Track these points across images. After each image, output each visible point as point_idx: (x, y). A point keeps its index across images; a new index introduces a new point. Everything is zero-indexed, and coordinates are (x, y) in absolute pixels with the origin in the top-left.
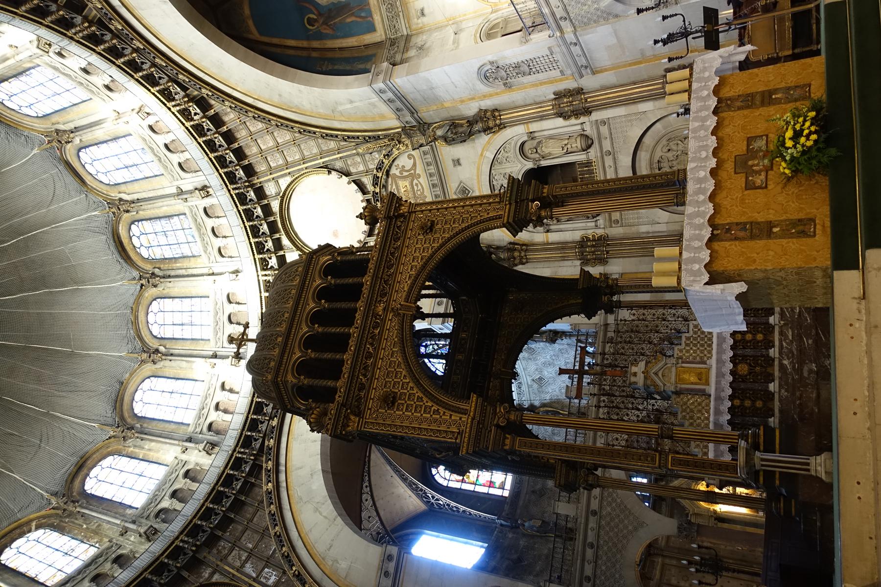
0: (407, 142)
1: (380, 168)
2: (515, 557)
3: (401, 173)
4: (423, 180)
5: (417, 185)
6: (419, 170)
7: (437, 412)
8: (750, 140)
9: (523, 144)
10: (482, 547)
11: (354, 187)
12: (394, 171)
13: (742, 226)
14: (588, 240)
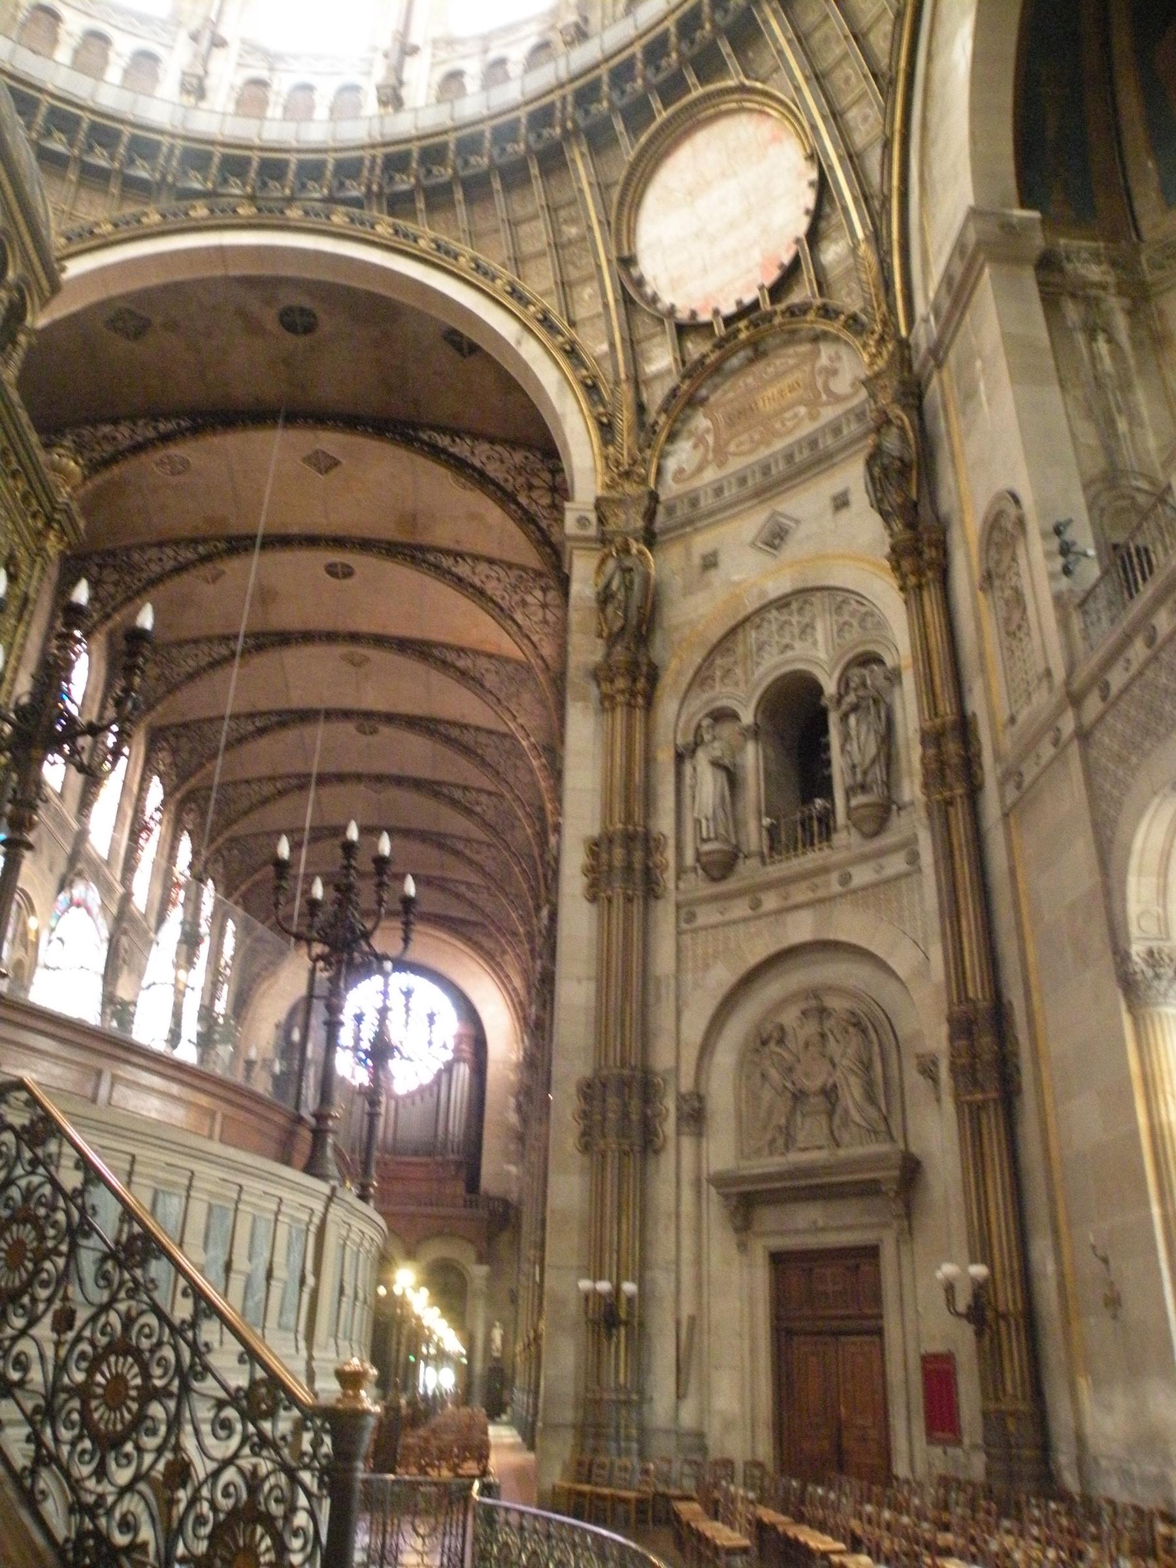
0: (881, 363)
6: (829, 413)
9: (869, 660)
11: (786, 259)
12: (826, 351)
14: (648, 853)
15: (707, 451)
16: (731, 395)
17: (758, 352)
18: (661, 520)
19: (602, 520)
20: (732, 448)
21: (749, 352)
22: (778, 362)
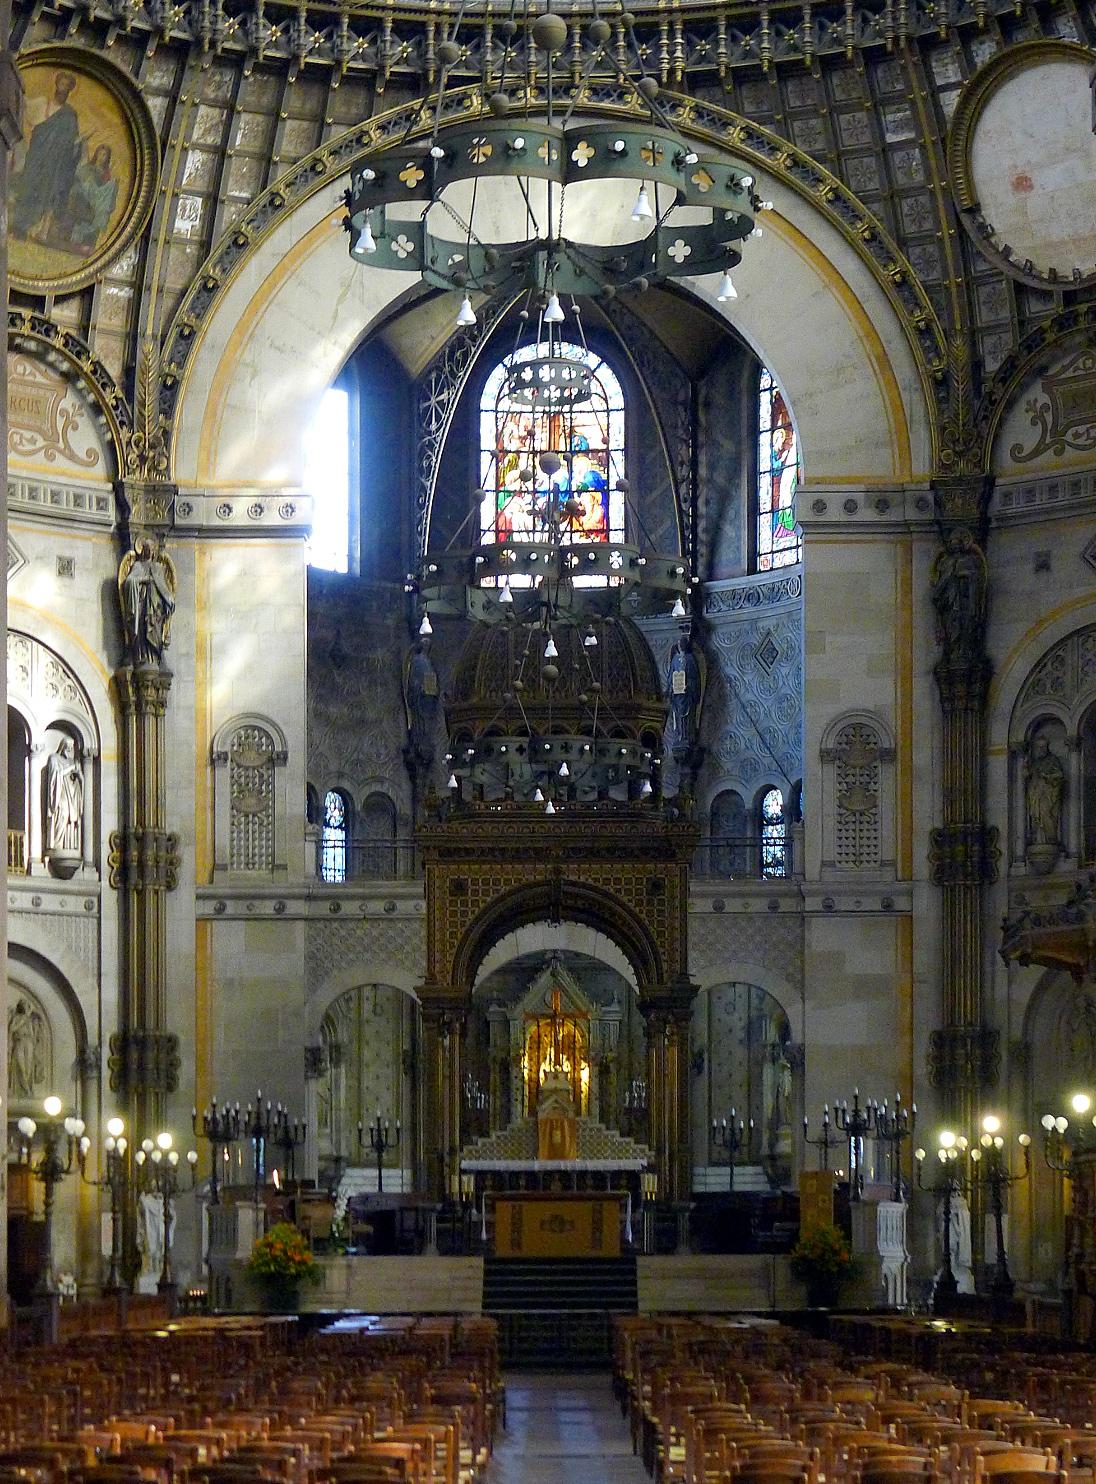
2: (346, 647)
7: (452, 946)
8: (572, 1222)
10: (351, 558)
13: (520, 1219)
15: (1044, 431)
16: (1069, 374)
18: (996, 506)
19: (938, 503)
20: (1069, 437)
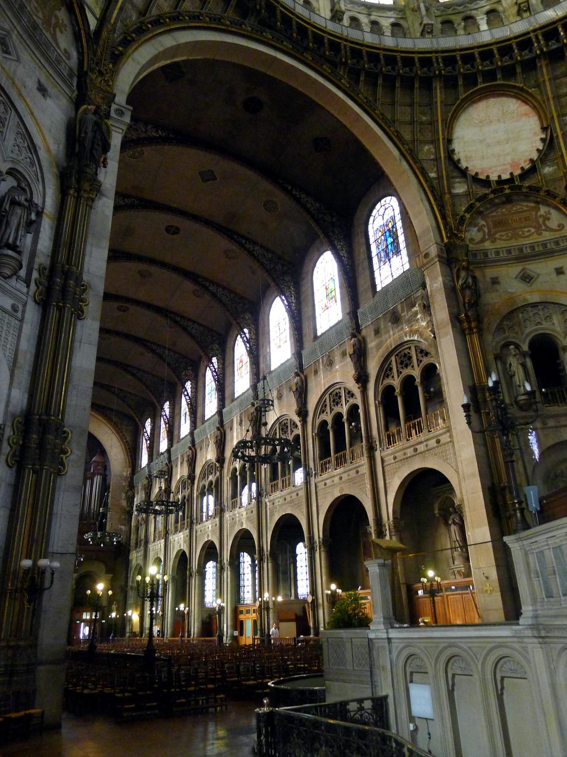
1: (548, 194)
3: (541, 216)
4: (535, 238)
5: (529, 231)
6: (547, 235)
15: (484, 235)
17: (509, 200)
20: (497, 236)
21: (504, 199)
22: (519, 207)
